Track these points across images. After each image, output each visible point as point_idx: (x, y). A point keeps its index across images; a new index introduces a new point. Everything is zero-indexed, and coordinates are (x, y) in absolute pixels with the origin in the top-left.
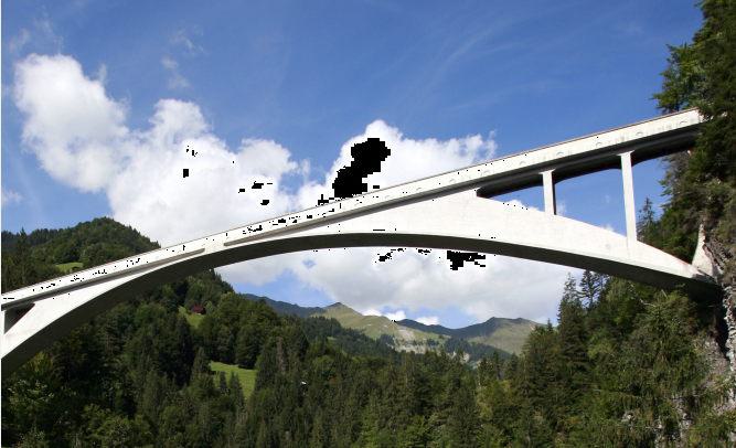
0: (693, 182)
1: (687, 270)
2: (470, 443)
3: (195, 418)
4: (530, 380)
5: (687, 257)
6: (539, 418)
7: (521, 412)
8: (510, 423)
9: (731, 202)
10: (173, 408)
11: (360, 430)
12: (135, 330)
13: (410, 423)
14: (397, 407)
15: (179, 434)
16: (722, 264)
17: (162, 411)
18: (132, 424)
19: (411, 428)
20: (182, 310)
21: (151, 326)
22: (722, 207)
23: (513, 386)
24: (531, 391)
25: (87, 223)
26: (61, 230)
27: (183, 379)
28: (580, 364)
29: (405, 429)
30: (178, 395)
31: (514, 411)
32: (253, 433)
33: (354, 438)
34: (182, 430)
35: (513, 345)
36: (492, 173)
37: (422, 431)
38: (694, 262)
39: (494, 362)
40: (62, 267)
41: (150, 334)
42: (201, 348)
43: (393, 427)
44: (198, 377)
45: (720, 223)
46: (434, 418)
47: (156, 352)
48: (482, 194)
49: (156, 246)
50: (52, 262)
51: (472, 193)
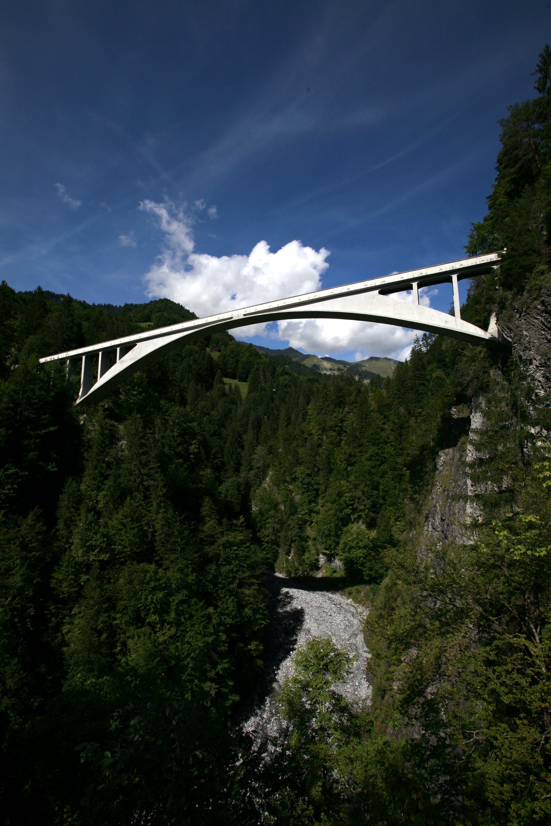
0: (490, 290)
1: (486, 335)
2: (366, 423)
3: (215, 408)
4: (397, 390)
5: (485, 327)
6: (402, 410)
7: (393, 406)
8: (387, 412)
9: (509, 301)
10: (203, 403)
11: (306, 415)
12: (183, 360)
13: (334, 412)
14: (327, 404)
15: (207, 416)
16: (506, 333)
17: (198, 404)
18: (185, 411)
19: (335, 415)
20: (208, 349)
21: (191, 358)
22: (504, 304)
23: (388, 393)
24: (397, 396)
25: (155, 301)
26: (141, 304)
27: (209, 387)
28: (422, 382)
29: (331, 415)
30: (207, 396)
31: (389, 406)
32: (247, 416)
33: (304, 420)
34: (208, 414)
35: (388, 373)
36: (386, 283)
37: (341, 416)
38: (488, 331)
39: (376, 380)
40: (144, 325)
41: (191, 362)
42: (219, 370)
43: (325, 414)
44: (217, 386)
45: (504, 312)
46: (346, 409)
47: (194, 372)
48: (380, 293)
49: (193, 317)
50: (136, 322)
51: (377, 292)
